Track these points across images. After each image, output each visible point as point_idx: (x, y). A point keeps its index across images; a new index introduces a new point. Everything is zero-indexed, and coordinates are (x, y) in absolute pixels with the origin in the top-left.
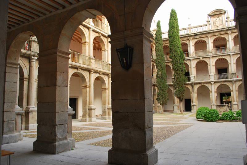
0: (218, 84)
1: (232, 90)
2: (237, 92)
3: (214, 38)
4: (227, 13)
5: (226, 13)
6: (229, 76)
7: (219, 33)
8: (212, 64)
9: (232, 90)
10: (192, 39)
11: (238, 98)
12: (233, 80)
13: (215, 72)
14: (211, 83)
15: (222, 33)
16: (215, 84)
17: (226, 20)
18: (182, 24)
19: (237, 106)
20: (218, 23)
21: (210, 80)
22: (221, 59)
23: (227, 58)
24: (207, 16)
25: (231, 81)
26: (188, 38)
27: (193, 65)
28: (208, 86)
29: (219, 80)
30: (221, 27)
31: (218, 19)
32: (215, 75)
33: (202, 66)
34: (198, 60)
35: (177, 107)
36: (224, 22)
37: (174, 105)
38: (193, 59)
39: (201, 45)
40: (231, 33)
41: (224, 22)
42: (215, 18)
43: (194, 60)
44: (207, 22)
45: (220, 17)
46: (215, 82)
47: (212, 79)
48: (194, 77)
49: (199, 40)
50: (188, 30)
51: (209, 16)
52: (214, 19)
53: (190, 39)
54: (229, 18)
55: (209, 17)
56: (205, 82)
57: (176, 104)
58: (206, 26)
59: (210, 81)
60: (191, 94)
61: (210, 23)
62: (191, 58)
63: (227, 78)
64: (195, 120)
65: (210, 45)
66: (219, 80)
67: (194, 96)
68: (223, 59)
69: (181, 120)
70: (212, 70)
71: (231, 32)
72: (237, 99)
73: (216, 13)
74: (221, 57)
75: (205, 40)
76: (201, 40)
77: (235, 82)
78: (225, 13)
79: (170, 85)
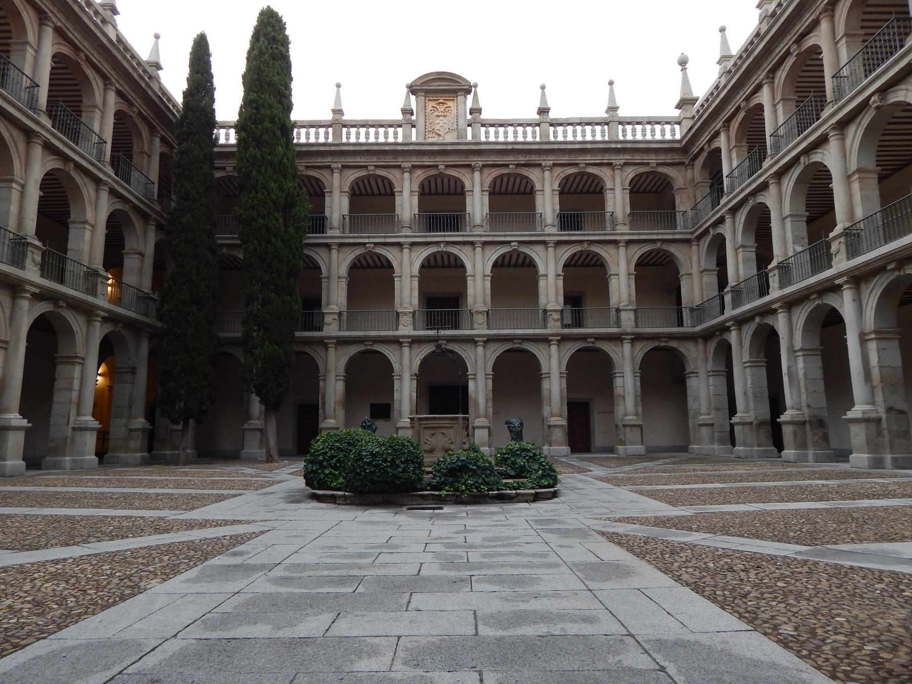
0: (427, 349)
1: (475, 375)
2: (490, 382)
3: (420, 175)
4: (476, 95)
5: (472, 94)
6: (464, 319)
8: (407, 267)
9: (475, 375)
10: (343, 167)
11: (490, 404)
12: (480, 336)
13: (416, 301)
14: (401, 343)
16: (416, 346)
17: (469, 117)
18: (309, 104)
19: (486, 431)
21: (397, 329)
22: (442, 254)
23: (464, 254)
24: (406, 90)
25: (471, 341)
26: (329, 159)
27: (337, 267)
28: (388, 351)
29: (432, 333)
30: (450, 138)
31: (441, 108)
32: (417, 315)
33: (371, 278)
34: (359, 251)
35: (259, 434)
36: (462, 123)
37: (246, 426)
38: (341, 245)
39: (372, 198)
40: (484, 166)
41: (462, 123)
42: (433, 104)
43: (344, 249)
45: (450, 104)
46: (416, 341)
47: (406, 329)
48: (340, 314)
49: (368, 177)
50: (330, 130)
51: (413, 89)
52: (430, 105)
53: (333, 165)
54: (479, 111)
55: (413, 98)
56: (379, 336)
57: (256, 423)
58: (400, 126)
60: (321, 384)
61: (414, 118)
62: (332, 237)
63: (457, 327)
64: (294, 498)
65: (407, 204)
66: (432, 333)
67: (334, 388)
68: (449, 254)
69: (220, 499)
70: (407, 292)
71: (481, 163)
72: (486, 408)
74: (442, 248)
75: (390, 177)
76: (377, 177)
77: (485, 342)
78: (468, 92)
79: (232, 342)
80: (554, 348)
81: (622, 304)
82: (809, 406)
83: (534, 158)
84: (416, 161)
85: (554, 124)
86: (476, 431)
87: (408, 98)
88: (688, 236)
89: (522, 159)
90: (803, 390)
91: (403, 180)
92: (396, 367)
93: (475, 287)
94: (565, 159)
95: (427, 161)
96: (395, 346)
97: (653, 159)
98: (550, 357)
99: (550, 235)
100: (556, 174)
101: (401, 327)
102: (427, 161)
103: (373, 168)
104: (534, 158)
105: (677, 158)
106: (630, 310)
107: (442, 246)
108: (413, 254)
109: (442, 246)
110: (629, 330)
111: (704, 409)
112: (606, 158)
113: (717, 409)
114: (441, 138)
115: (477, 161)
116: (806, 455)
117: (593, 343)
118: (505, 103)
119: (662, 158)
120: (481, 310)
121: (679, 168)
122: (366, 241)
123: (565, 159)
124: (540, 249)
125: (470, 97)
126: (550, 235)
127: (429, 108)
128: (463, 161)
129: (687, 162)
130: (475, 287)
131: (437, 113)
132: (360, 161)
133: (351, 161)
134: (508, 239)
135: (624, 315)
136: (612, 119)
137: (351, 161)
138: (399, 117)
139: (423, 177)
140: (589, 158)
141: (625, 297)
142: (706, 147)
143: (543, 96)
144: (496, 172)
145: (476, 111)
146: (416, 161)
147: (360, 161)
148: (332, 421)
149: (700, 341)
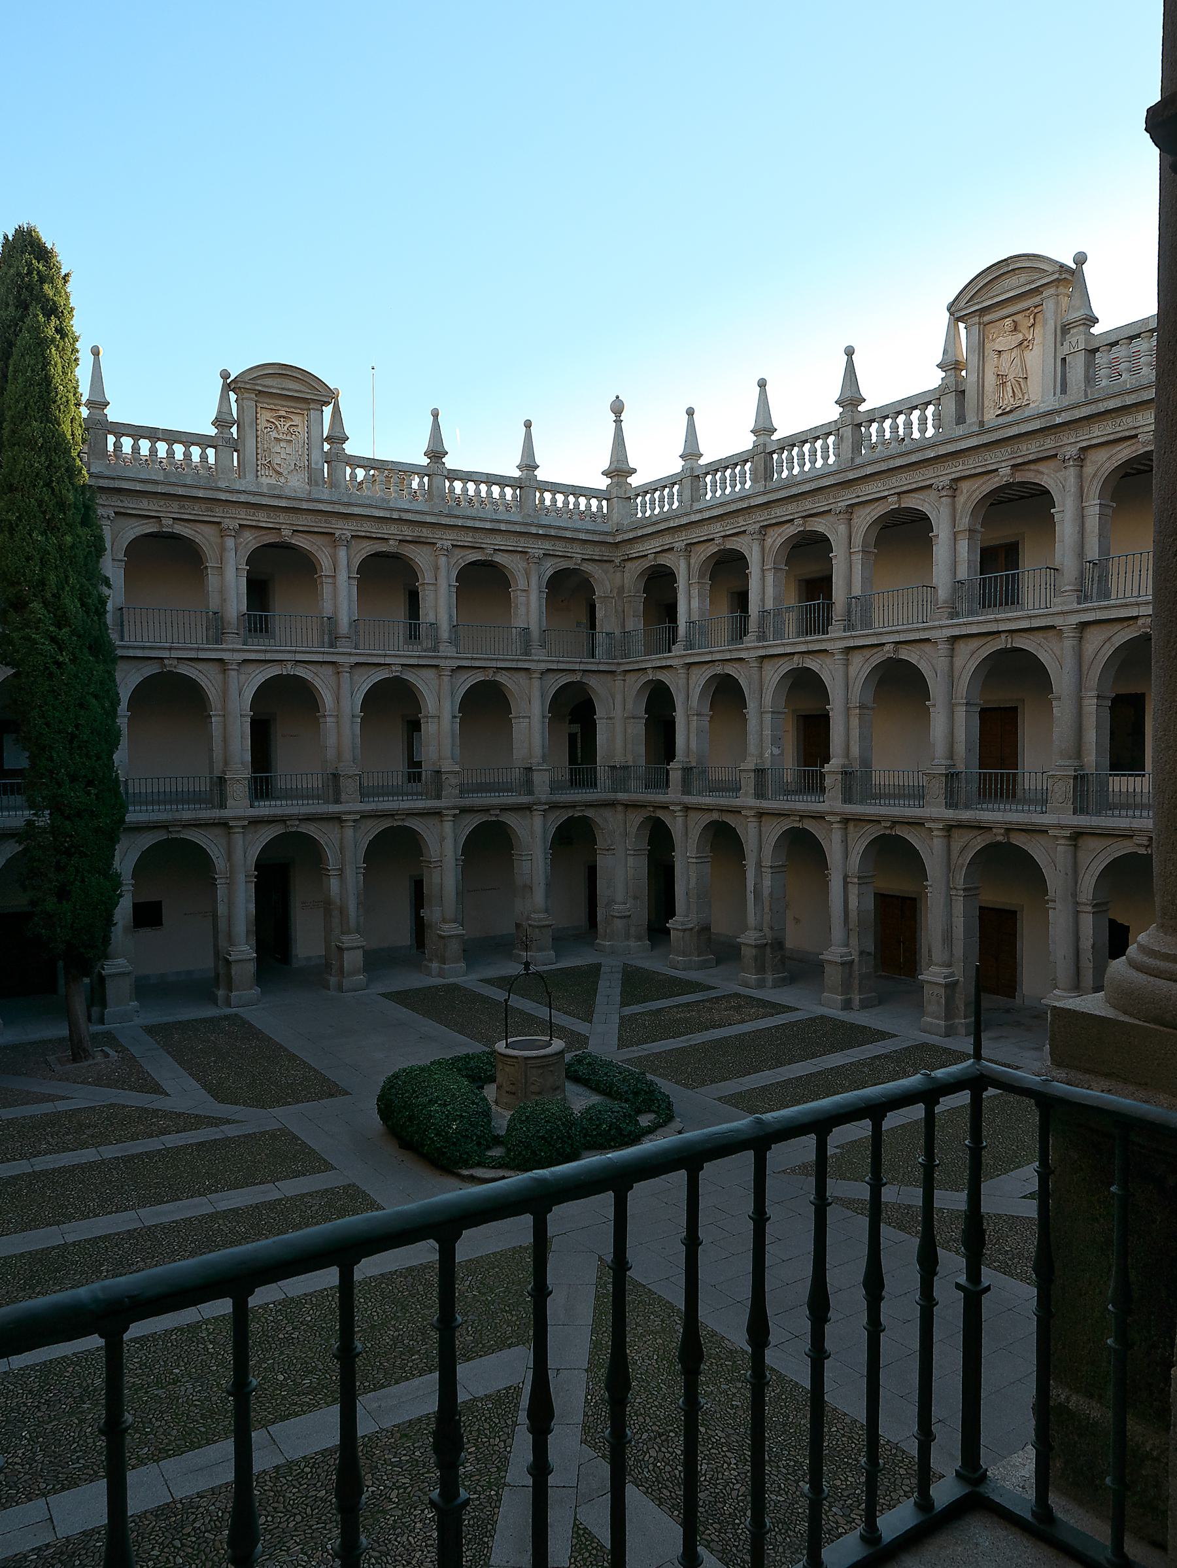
1: (341, 870)
3: (251, 541)
7: (282, 518)
12: (350, 813)
15: (303, 521)
20: (283, 455)
30: (296, 484)
31: (283, 426)
36: (316, 456)
42: (267, 415)
44: (217, 423)
45: (297, 420)
55: (233, 396)
59: (226, 813)
73: (274, 385)
74: (289, 670)
80: (448, 826)
81: (534, 761)
82: (772, 928)
83: (426, 532)
84: (245, 517)
85: (454, 475)
86: (346, 955)
87: (224, 398)
88: (613, 668)
89: (408, 532)
90: (767, 910)
91: (223, 549)
92: (220, 863)
93: (339, 734)
94: (468, 539)
95: (262, 519)
96: (218, 831)
97: (577, 552)
98: (442, 839)
99: (446, 658)
100: (453, 561)
101: (230, 802)
102: (262, 519)
103: (171, 522)
104: (426, 532)
105: (607, 553)
106: (546, 770)
107: (289, 666)
108: (243, 677)
109: (289, 666)
110: (544, 798)
111: (620, 897)
112: (522, 543)
113: (635, 898)
114: (282, 480)
115: (343, 529)
116: (763, 980)
117: (497, 815)
118: (380, 430)
119: (590, 551)
120: (351, 773)
121: (606, 565)
122: (165, 654)
123: (468, 539)
124: (430, 674)
125: (328, 411)
126: (446, 658)
127: (262, 424)
128: (322, 525)
129: (617, 561)
130: (339, 734)
131: (274, 434)
132: (145, 506)
133: (130, 505)
134: (388, 660)
135: (537, 778)
136: (527, 481)
137: (130, 505)
138: (212, 431)
139: (254, 545)
140: (499, 541)
141: (538, 751)
142: (651, 557)
143: (436, 427)
144: (368, 548)
145: (338, 438)
146: (245, 517)
147: (145, 506)
148: (121, 961)
149: (620, 808)
